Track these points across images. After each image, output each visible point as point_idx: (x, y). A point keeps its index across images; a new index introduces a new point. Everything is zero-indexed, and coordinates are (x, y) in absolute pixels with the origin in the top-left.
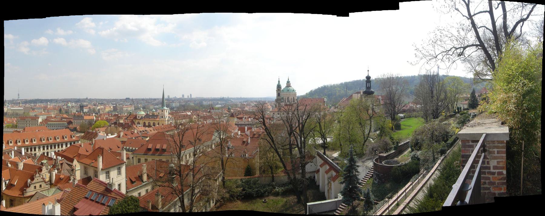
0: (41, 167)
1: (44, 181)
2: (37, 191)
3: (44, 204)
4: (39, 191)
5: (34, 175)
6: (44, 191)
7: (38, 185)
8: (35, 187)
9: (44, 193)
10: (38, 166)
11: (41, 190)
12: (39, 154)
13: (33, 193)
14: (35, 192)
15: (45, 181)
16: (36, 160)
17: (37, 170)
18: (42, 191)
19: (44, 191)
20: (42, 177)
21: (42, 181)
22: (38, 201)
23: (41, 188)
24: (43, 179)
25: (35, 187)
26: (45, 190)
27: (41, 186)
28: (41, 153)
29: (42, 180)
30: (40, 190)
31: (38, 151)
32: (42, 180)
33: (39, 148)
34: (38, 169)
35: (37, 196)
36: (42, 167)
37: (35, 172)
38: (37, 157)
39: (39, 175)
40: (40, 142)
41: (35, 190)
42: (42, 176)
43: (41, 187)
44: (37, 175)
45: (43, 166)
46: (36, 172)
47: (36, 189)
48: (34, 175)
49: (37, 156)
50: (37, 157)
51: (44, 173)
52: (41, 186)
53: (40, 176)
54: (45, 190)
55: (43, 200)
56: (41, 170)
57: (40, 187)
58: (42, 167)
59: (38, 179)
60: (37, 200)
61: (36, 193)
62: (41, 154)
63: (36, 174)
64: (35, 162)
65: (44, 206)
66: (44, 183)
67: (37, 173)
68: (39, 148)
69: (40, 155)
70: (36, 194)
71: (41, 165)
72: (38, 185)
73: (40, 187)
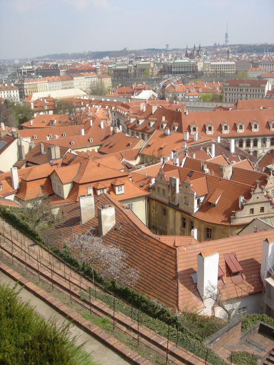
0: (266, 177)
1: (269, 201)
2: (255, 217)
3: (267, 240)
4: (258, 217)
5: (253, 189)
6: (267, 218)
7: (257, 208)
8: (252, 211)
9: (268, 222)
10: (260, 173)
11: (263, 216)
12: (263, 152)
13: (248, 220)
14: (252, 219)
15: (271, 201)
16: (257, 163)
17: (258, 181)
18: (265, 218)
19: (267, 218)
20: (265, 193)
21: (266, 202)
22: (256, 234)
23: (263, 213)
24: (269, 198)
25: (252, 211)
26: (269, 217)
27: (262, 209)
28: (266, 151)
29: (266, 199)
30: (261, 216)
31: (262, 146)
32: (266, 199)
33: (264, 141)
34: (259, 180)
35: (254, 225)
36: (268, 176)
37: (253, 185)
38: (259, 158)
39: (260, 190)
40: (267, 130)
41: (252, 215)
42: (267, 192)
43: (263, 211)
44: (258, 190)
45: (270, 174)
46: (255, 184)
47: (253, 213)
48: (253, 189)
49: (258, 156)
50: (259, 158)
51: (270, 188)
52: (262, 209)
53: (262, 192)
54: (269, 217)
55: (265, 233)
56: (265, 182)
57: (261, 212)
58: (268, 176)
59: (258, 198)
60: (255, 232)
61: (254, 220)
62: (268, 153)
63: (255, 188)
64: (255, 166)
65: (266, 243)
66: (269, 204)
67: (258, 186)
68: (264, 141)
69: (264, 154)
70: (253, 222)
71: (265, 172)
72: (257, 208)
73: (261, 212)
